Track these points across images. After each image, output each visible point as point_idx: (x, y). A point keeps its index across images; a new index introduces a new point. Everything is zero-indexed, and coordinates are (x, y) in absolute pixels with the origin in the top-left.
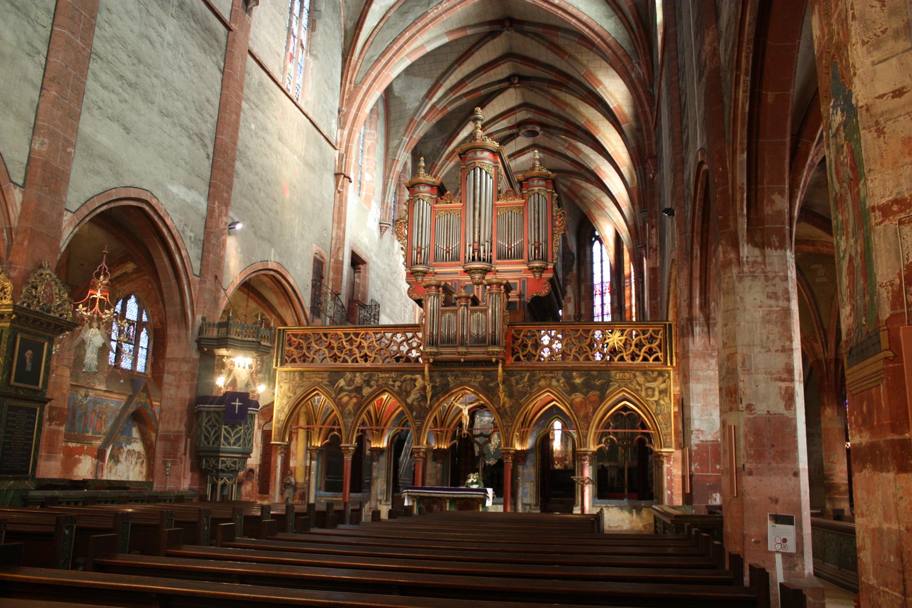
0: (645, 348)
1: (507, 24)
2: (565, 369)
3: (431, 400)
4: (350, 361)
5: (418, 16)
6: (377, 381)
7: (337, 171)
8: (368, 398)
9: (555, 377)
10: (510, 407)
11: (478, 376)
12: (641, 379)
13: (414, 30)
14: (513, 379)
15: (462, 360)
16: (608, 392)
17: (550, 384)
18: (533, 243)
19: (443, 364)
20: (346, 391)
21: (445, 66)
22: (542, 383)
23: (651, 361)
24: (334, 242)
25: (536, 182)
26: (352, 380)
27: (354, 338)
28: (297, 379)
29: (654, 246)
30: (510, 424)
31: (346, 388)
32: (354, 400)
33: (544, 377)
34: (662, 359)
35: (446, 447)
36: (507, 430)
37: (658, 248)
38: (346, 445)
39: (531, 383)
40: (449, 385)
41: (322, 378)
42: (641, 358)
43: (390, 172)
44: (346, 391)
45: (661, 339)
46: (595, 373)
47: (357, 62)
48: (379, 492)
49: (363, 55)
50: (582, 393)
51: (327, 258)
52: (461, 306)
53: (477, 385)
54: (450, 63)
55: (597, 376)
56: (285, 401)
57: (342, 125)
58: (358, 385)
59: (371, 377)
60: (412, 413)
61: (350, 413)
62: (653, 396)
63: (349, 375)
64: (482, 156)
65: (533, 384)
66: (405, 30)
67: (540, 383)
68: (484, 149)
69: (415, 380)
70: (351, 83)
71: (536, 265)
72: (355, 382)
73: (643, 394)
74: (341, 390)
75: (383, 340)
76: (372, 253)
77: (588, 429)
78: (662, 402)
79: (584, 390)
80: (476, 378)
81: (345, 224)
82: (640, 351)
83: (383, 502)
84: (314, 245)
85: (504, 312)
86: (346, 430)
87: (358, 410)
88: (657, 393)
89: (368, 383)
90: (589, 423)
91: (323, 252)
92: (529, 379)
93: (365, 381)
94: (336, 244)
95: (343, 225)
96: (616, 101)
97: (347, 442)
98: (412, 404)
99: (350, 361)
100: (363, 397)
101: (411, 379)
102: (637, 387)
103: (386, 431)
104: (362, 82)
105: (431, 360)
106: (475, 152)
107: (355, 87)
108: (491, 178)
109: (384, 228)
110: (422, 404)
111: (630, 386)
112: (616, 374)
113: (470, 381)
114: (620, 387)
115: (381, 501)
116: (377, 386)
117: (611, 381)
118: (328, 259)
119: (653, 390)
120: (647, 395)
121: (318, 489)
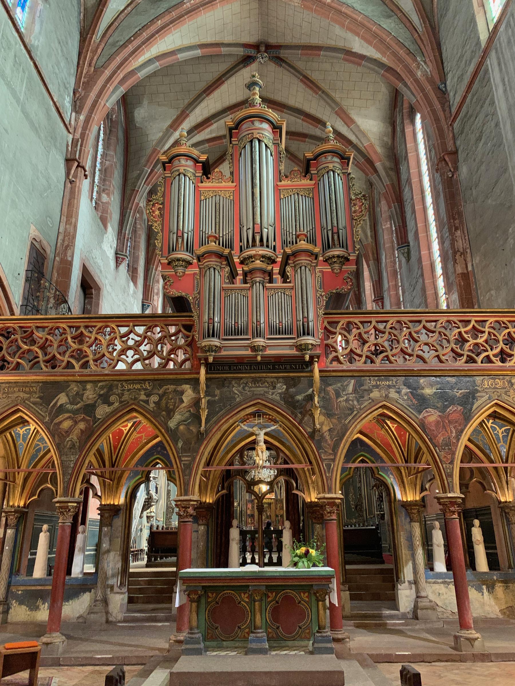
1: (263, 49)
2: (409, 374)
3: (206, 423)
4: (77, 366)
5: (172, 4)
6: (121, 396)
7: (69, 156)
8: (104, 421)
9: (394, 386)
13: (167, 19)
14: (330, 389)
15: (259, 358)
16: (474, 407)
17: (387, 396)
18: (329, 227)
19: (226, 368)
20: (68, 411)
21: (192, 96)
22: (375, 394)
25: (330, 158)
26: (79, 395)
27: (86, 333)
30: (332, 457)
32: (82, 426)
33: (377, 386)
35: (211, 501)
36: (329, 466)
38: (63, 499)
40: (235, 399)
41: (30, 393)
43: (129, 202)
44: (68, 411)
46: (453, 380)
47: (99, 45)
48: (110, 573)
49: (106, 39)
53: (278, 398)
54: (197, 93)
55: (456, 384)
57: (77, 107)
58: (89, 402)
59: (110, 388)
60: (176, 443)
61: (73, 446)
63: (74, 388)
64: (261, 126)
66: (157, 18)
67: (372, 395)
68: (264, 119)
69: (182, 393)
70: (90, 65)
71: (337, 253)
74: (61, 409)
75: (132, 336)
76: (107, 281)
77: (452, 462)
80: (274, 388)
81: (77, 220)
83: (116, 589)
84: (33, 227)
87: (86, 442)
89: (105, 399)
90: (453, 454)
91: (45, 243)
92: (355, 391)
93: (100, 396)
96: (369, 140)
97: (65, 493)
98: (177, 428)
99: (77, 366)
100: (95, 420)
101: (175, 391)
103: (124, 480)
104: (104, 66)
106: (252, 122)
107: (95, 70)
108: (271, 155)
109: (120, 260)
110: (193, 429)
111: (506, 398)
113: (266, 392)
115: (112, 587)
116: (121, 402)
117: (477, 391)
118: (52, 256)
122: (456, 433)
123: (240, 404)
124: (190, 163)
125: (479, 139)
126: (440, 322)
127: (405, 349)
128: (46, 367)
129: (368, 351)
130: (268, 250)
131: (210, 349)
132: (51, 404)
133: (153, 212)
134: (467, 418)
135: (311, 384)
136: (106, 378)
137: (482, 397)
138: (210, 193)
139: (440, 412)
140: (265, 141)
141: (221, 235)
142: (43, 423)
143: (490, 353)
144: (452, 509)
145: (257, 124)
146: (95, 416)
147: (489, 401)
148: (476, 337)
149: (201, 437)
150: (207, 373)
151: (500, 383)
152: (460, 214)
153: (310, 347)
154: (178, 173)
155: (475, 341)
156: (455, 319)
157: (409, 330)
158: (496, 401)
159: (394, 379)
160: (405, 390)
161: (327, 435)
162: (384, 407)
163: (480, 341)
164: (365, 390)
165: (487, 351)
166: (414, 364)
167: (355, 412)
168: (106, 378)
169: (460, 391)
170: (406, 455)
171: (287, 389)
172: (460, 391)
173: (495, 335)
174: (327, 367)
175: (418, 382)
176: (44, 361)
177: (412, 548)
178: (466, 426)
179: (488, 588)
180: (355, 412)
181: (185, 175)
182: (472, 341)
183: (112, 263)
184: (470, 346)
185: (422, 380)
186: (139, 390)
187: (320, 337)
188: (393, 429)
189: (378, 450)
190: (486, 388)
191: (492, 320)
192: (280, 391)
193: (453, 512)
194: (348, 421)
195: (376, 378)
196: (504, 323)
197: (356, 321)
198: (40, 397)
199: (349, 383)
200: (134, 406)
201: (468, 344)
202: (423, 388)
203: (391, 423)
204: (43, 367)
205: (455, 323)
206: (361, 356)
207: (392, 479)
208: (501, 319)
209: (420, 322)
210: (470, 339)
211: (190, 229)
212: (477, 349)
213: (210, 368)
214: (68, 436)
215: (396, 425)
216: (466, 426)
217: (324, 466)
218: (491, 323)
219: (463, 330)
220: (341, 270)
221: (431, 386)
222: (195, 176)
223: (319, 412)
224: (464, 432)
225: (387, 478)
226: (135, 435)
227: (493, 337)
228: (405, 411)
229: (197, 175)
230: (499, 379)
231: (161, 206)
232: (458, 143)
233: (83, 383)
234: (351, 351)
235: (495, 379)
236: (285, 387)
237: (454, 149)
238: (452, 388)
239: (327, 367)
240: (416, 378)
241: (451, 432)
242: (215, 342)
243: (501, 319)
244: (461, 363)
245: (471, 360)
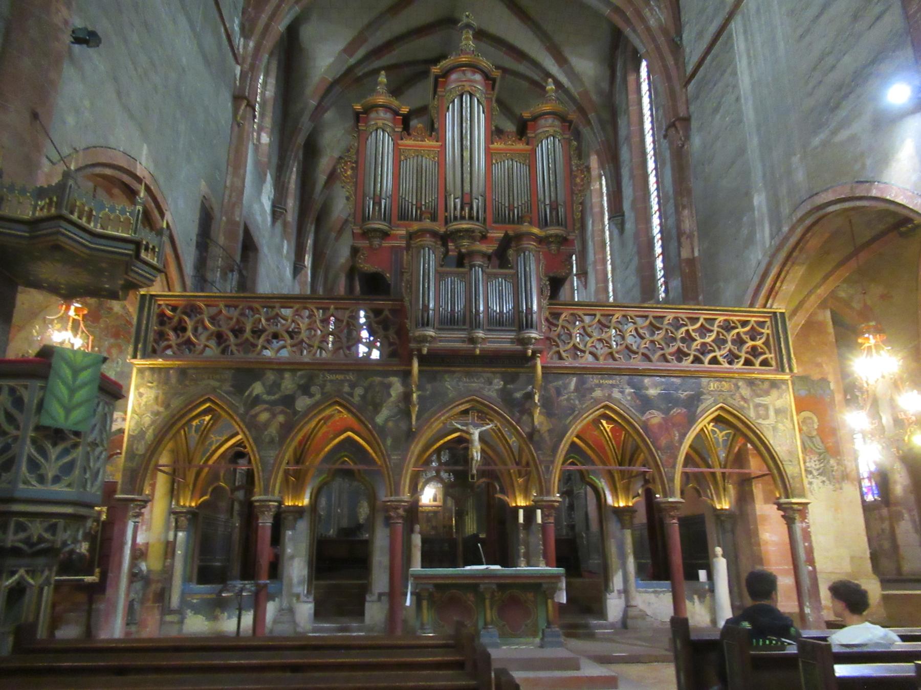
0: (747, 345)
2: (635, 372)
3: (418, 418)
6: (322, 387)
10: (550, 431)
11: (496, 381)
12: (745, 391)
15: (478, 352)
16: (699, 410)
17: (610, 396)
18: (547, 202)
22: (598, 393)
23: (757, 367)
24: (227, 192)
28: (173, 380)
29: (688, 231)
31: (265, 397)
32: (281, 418)
33: (599, 385)
34: (773, 363)
36: (547, 468)
37: (696, 233)
39: (583, 391)
42: (742, 361)
45: (768, 334)
46: (677, 381)
48: (295, 580)
50: (658, 409)
51: (217, 213)
52: (474, 266)
53: (494, 394)
56: (147, 420)
58: (288, 393)
59: (311, 380)
61: (272, 441)
62: (767, 417)
63: (271, 377)
64: (472, 78)
65: (584, 396)
69: (389, 386)
72: (283, 387)
73: (752, 414)
74: (257, 400)
77: (674, 466)
78: (780, 426)
79: (663, 406)
80: (491, 383)
82: (739, 350)
83: (303, 598)
85: (541, 279)
86: (263, 471)
88: (772, 413)
89: (305, 390)
90: (676, 457)
92: (577, 389)
94: (230, 196)
95: (242, 172)
100: (295, 413)
101: (382, 383)
102: (742, 403)
105: (425, 351)
108: (484, 112)
112: (709, 383)
114: (716, 402)
115: (298, 596)
116: (323, 394)
117: (702, 394)
119: (766, 408)
120: (759, 416)
121: (187, 580)
122: (679, 436)
123: (453, 401)
124: (389, 115)
125: (716, 110)
126: (667, 318)
127: (630, 346)
128: (238, 351)
129: (592, 346)
130: (477, 223)
131: (424, 339)
132: (246, 394)
133: (346, 171)
134: (692, 419)
135: (531, 380)
136: (306, 367)
137: (707, 399)
138: (414, 153)
139: (663, 414)
140: (478, 95)
141: (423, 203)
142: (238, 415)
143: (717, 353)
144: (672, 513)
145: (469, 75)
146: (294, 409)
147: (713, 404)
148: (703, 336)
149: (411, 435)
150: (419, 365)
151: (726, 385)
152: (689, 192)
153: (533, 340)
154: (375, 128)
155: (703, 341)
156: (683, 316)
157: (635, 326)
158: (721, 405)
159: (618, 378)
160: (629, 390)
161: (546, 436)
162: (606, 407)
163: (708, 340)
164: (588, 389)
165: (714, 351)
166: (637, 363)
167: (577, 412)
168: (306, 367)
169: (686, 393)
170: (619, 457)
171: (505, 384)
172: (686, 393)
173: (723, 335)
174: (548, 363)
175: (643, 382)
176: (236, 345)
177: (623, 557)
178: (690, 429)
179: (699, 598)
180: (577, 412)
181: (384, 131)
182: (700, 341)
183: (269, 219)
184: (697, 346)
185: (647, 381)
186: (342, 381)
187: (544, 330)
188: (608, 430)
189: (589, 452)
190: (712, 391)
191: (721, 318)
192: (497, 387)
193: (673, 518)
194: (568, 421)
195: (600, 376)
196: (733, 322)
197: (580, 313)
198: (232, 386)
199: (571, 380)
200: (338, 400)
201: (695, 343)
202: (647, 389)
203: (607, 423)
204: (235, 352)
205: (683, 320)
206: (583, 352)
207: (603, 484)
208: (731, 318)
209: (646, 317)
210: (698, 338)
211: (388, 195)
212: (704, 349)
213: (423, 360)
214: (266, 429)
215: (611, 426)
216: (690, 429)
217: (542, 468)
218: (720, 322)
219: (691, 328)
220: (558, 250)
221: (655, 386)
222: (395, 131)
223: (538, 411)
224: (688, 436)
225: (597, 481)
226: (324, 429)
227: (721, 337)
228: (628, 412)
229: (396, 130)
230: (726, 382)
231: (354, 165)
232: (692, 108)
233: (280, 372)
234: (574, 346)
235: (721, 381)
236: (502, 383)
237: (686, 115)
238: (677, 389)
239: (548, 363)
240: (640, 377)
241: (675, 436)
242: (431, 333)
243: (731, 318)
244: (687, 363)
245: (697, 360)
